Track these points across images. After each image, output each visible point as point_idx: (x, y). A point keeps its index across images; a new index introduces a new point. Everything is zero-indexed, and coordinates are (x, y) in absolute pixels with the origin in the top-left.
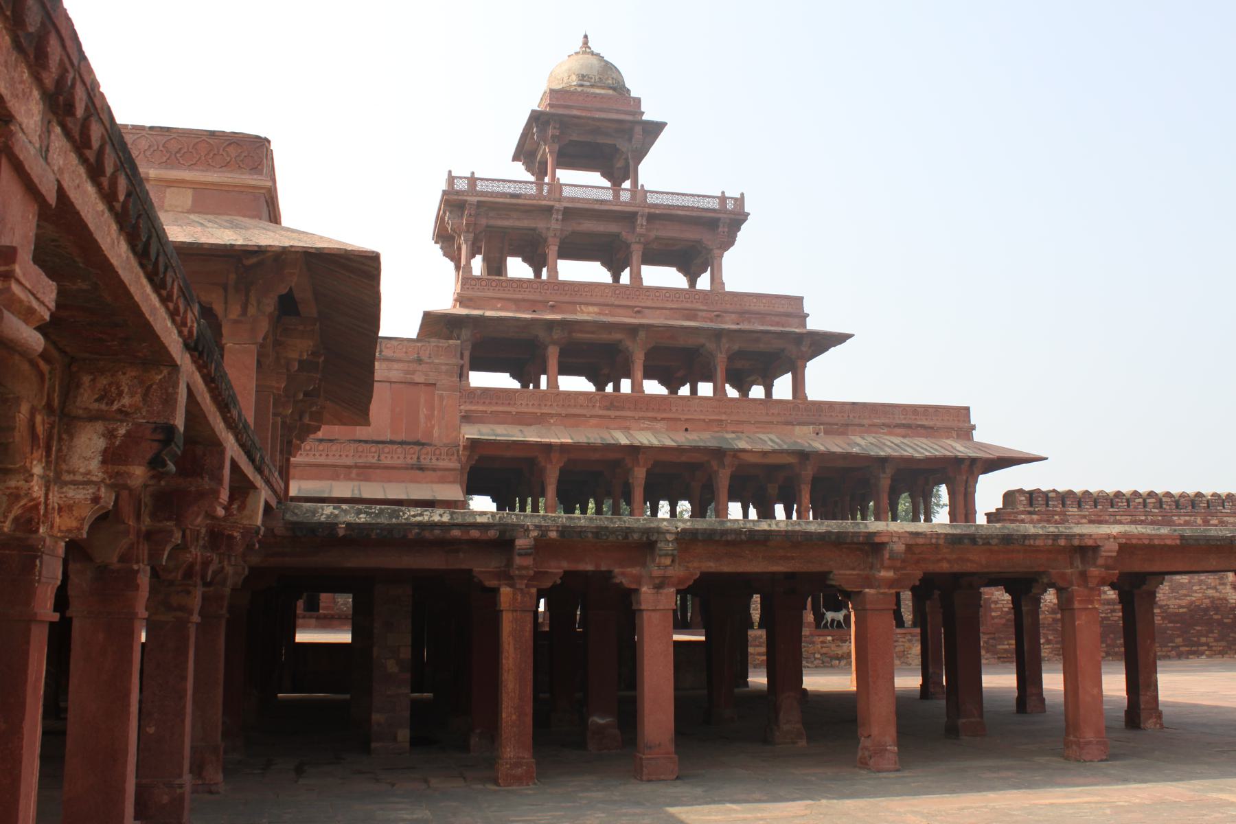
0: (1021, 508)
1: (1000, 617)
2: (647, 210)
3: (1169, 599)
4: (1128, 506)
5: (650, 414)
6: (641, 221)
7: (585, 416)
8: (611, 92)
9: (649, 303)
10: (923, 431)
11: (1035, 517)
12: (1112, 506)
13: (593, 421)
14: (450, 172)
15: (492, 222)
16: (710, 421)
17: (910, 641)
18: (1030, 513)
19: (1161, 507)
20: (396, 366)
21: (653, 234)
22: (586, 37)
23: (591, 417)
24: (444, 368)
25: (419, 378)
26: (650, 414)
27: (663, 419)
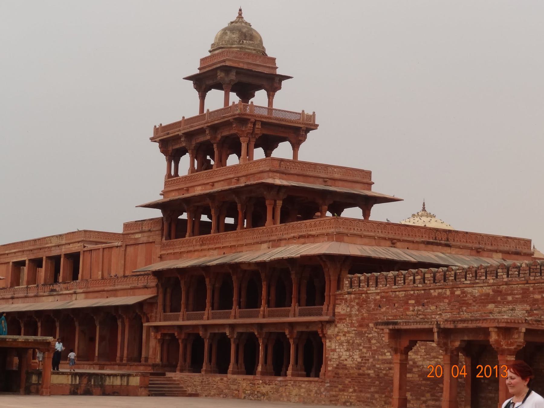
0: (346, 290)
1: (332, 371)
2: (206, 125)
3: (424, 360)
4: (404, 283)
5: (211, 246)
6: (207, 132)
7: (190, 251)
8: (220, 50)
9: (217, 179)
10: (312, 239)
11: (353, 296)
12: (395, 285)
13: (196, 253)
14: (155, 126)
15: (174, 148)
16: (231, 247)
17: (292, 385)
18: (349, 293)
19: (424, 282)
20: (145, 234)
21: (219, 137)
22: (240, 10)
23: (194, 251)
24: (157, 232)
25: (151, 241)
26: (211, 246)
27: (215, 249)
